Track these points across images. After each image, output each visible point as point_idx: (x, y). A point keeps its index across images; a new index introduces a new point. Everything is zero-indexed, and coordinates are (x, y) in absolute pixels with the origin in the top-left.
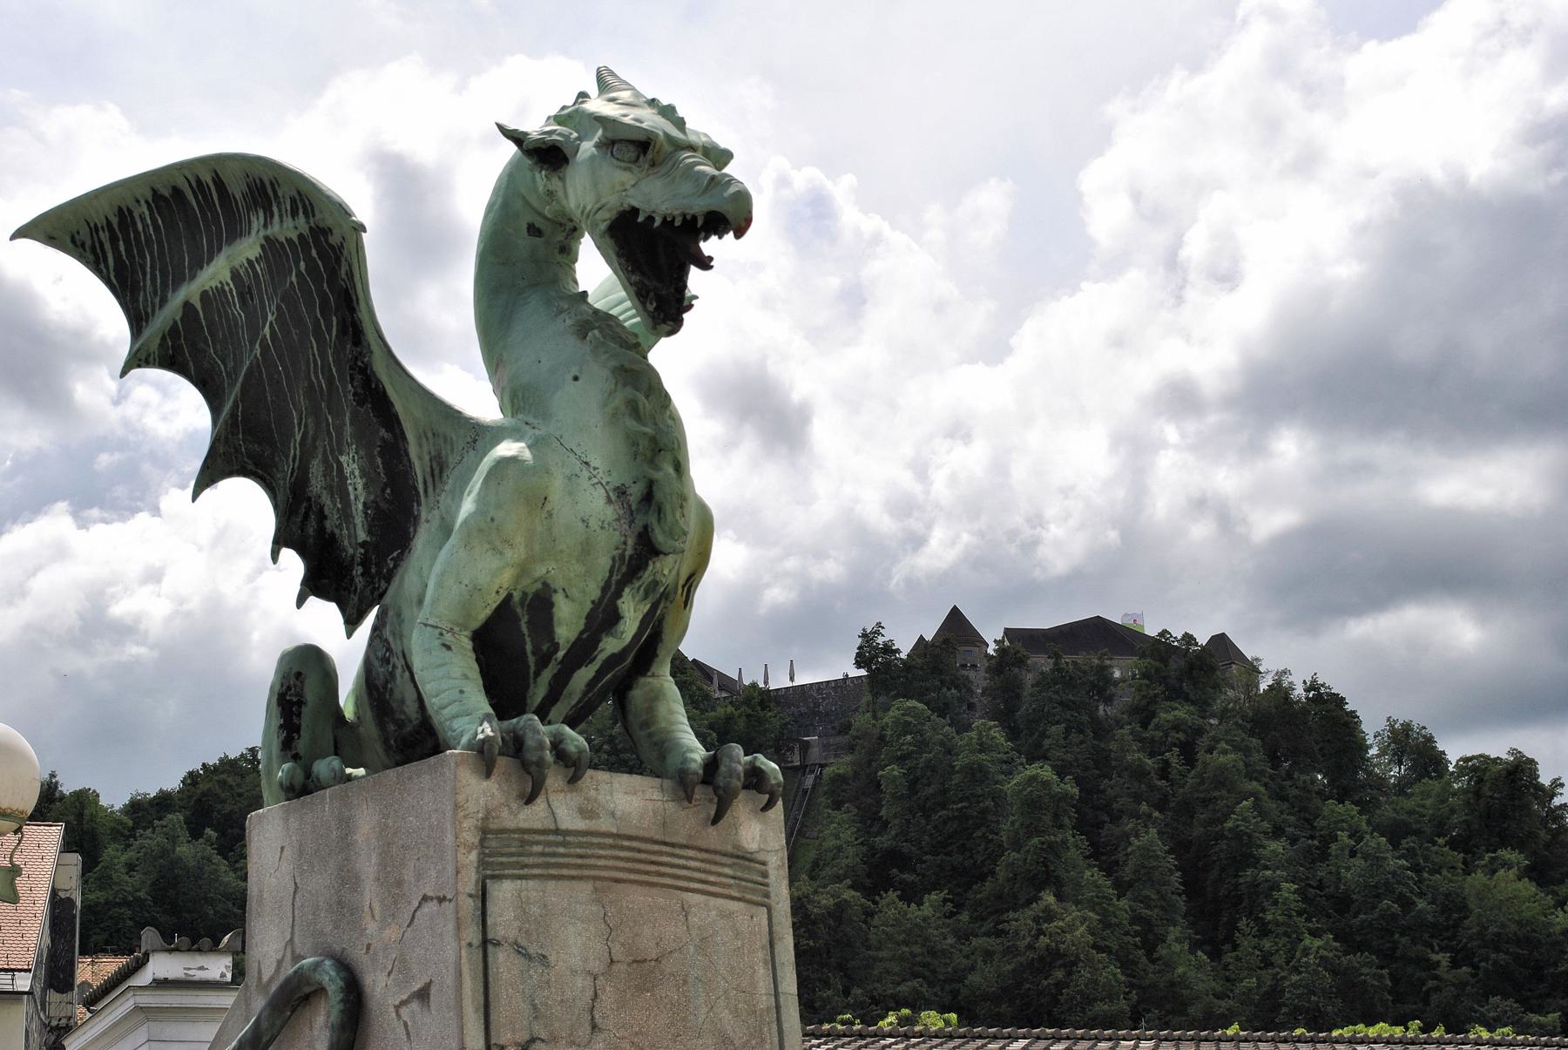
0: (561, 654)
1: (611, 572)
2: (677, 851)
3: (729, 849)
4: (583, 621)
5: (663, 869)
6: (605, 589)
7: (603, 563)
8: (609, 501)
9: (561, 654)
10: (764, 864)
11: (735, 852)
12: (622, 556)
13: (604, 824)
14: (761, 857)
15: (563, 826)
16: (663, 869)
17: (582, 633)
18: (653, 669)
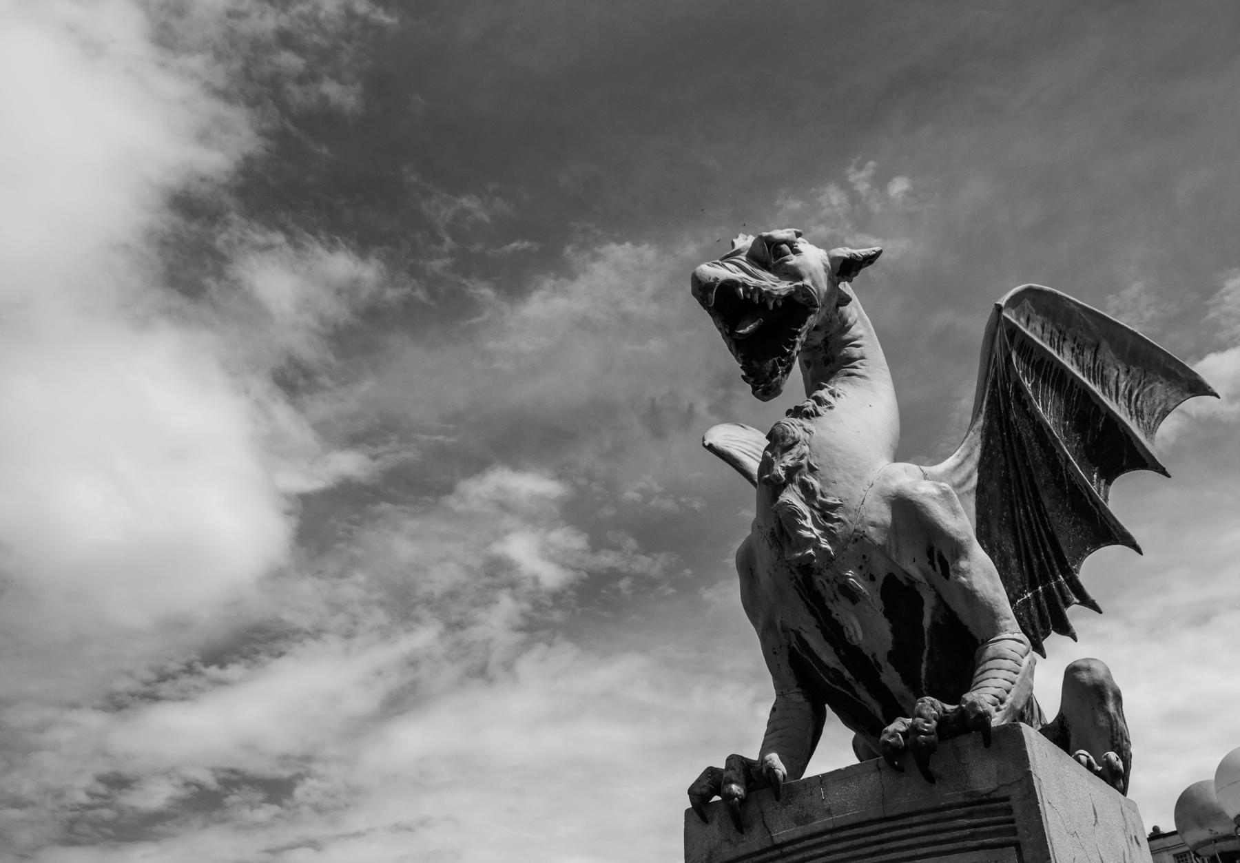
0: (847, 674)
1: (803, 599)
2: (900, 823)
3: (961, 799)
4: (827, 644)
5: (885, 846)
6: (812, 612)
7: (792, 594)
8: (771, 547)
9: (847, 674)
10: (1007, 799)
11: (968, 799)
12: (798, 582)
13: (818, 824)
14: (997, 795)
15: (778, 841)
16: (885, 846)
17: (837, 652)
18: (979, 636)
